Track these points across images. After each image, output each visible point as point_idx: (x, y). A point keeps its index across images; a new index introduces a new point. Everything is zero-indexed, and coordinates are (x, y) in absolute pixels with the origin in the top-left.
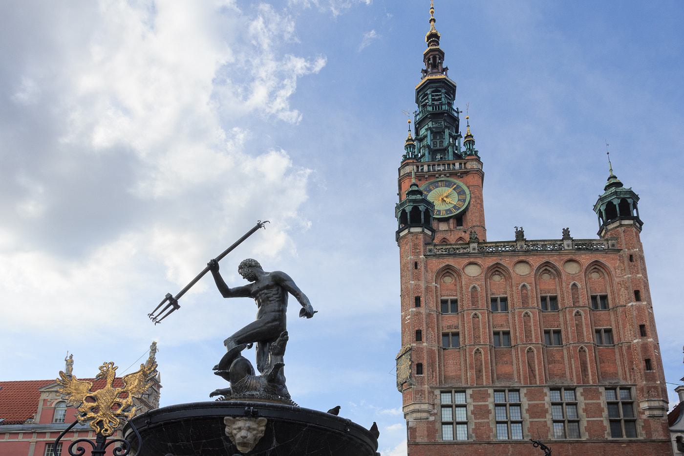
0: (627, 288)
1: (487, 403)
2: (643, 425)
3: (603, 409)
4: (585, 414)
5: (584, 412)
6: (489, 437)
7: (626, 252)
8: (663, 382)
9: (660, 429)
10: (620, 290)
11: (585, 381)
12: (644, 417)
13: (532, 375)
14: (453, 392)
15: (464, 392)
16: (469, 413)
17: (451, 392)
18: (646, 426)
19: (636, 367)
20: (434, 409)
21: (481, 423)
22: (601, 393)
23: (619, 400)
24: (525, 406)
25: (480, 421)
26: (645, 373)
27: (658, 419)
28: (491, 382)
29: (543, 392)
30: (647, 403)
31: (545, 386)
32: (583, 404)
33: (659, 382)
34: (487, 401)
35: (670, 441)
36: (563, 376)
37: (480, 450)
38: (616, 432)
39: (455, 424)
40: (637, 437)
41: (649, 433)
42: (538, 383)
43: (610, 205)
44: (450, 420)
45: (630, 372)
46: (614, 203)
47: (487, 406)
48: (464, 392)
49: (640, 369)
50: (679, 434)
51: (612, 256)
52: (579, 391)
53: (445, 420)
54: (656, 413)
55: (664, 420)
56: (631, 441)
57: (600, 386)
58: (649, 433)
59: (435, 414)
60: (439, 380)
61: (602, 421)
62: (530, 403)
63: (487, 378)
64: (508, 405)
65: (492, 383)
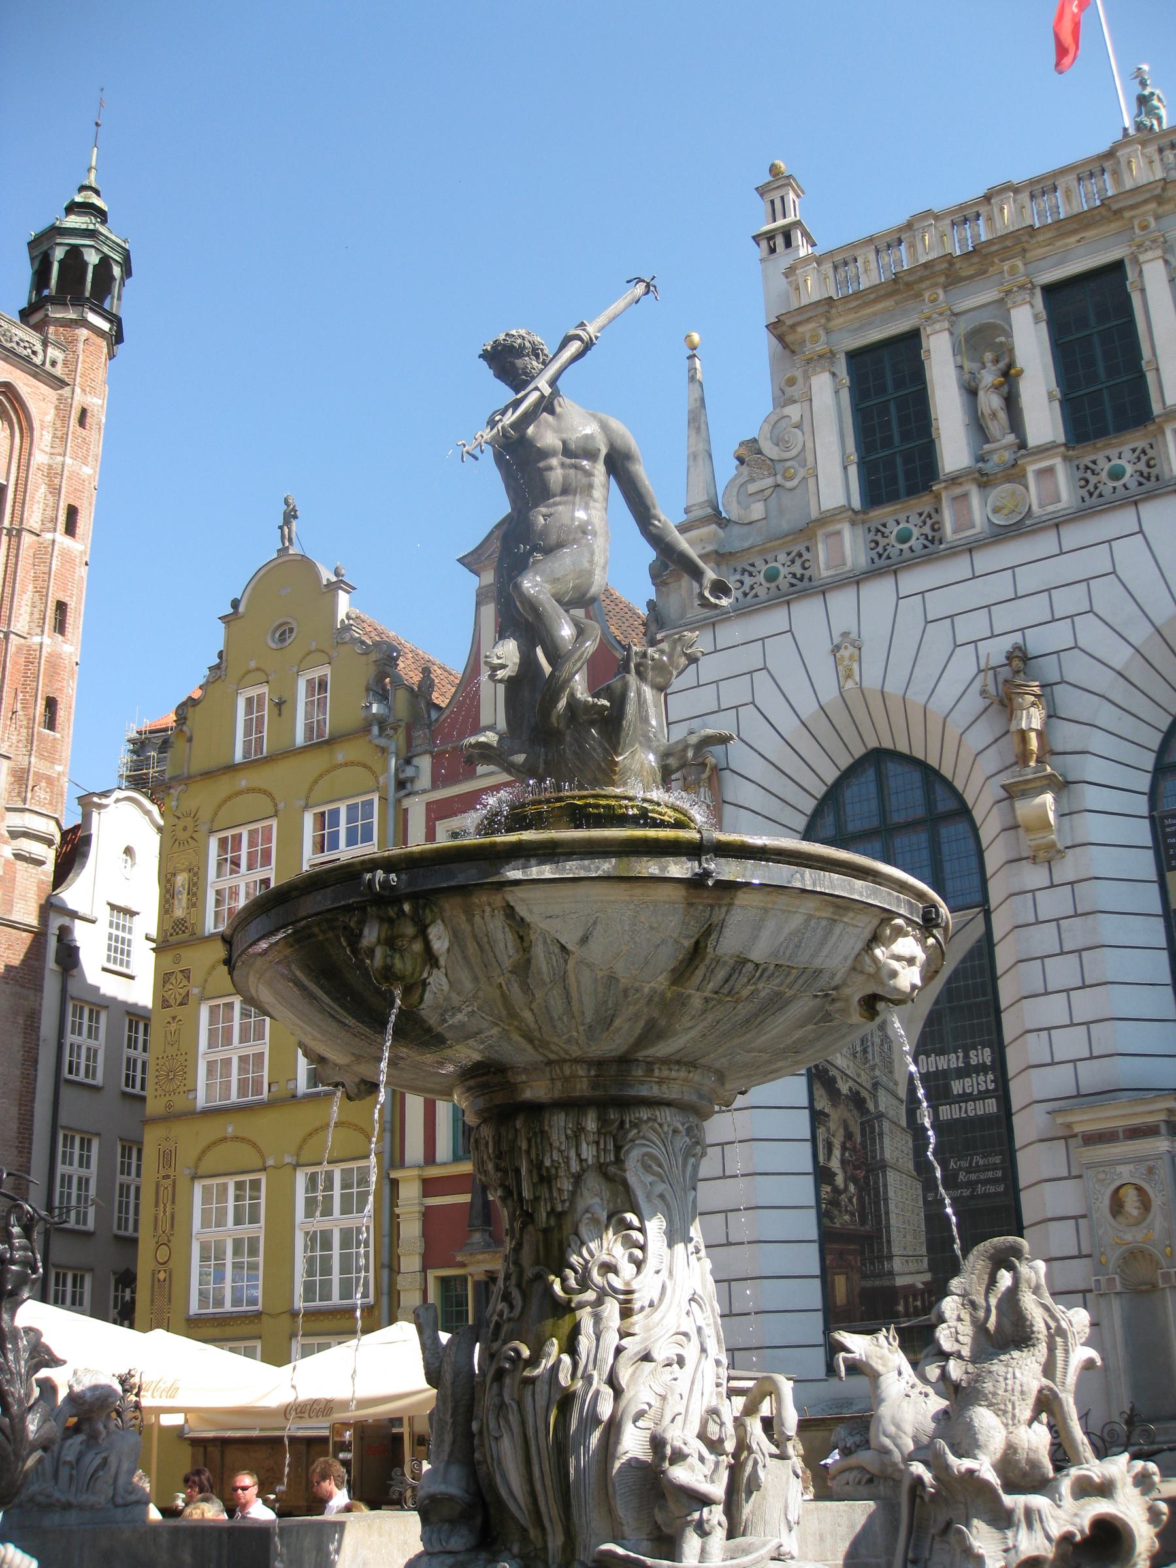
0: (56, 491)
7: (79, 399)
10: (37, 487)
33: (59, 768)
43: (75, 253)
46: (86, 258)
51: (44, 389)
55: (44, 873)
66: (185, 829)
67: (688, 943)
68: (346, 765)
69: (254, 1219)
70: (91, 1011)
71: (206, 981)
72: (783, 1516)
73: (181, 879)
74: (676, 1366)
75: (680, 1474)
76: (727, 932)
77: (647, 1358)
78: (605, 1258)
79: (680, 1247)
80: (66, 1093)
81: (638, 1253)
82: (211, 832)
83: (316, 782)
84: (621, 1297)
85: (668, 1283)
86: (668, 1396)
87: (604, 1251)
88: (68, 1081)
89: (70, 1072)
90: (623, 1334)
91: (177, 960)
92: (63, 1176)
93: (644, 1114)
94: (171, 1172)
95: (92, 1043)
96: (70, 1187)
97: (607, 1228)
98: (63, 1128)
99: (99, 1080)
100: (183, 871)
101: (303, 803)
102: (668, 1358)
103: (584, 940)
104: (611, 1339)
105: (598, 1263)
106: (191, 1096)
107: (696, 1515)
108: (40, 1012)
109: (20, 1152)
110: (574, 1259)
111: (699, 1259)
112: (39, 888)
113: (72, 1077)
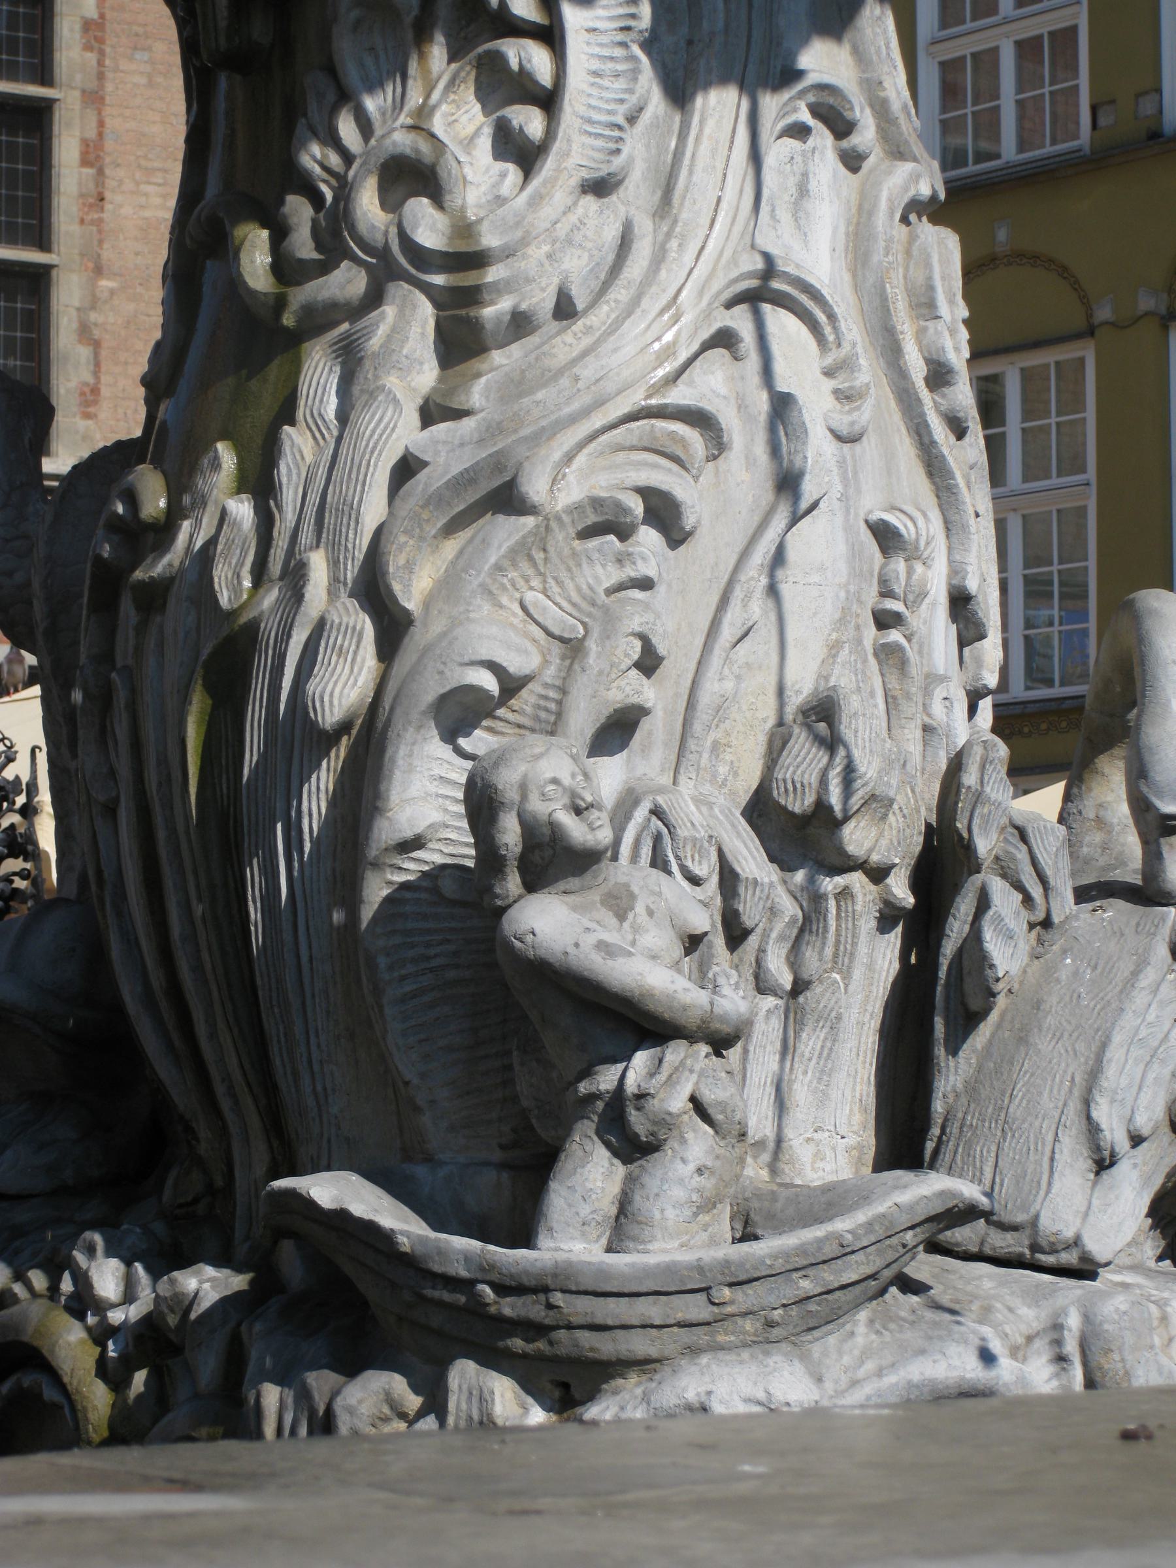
69: (1073, 463)
72: (1074, 1106)
74: (649, 538)
75: (548, 923)
77: (507, 499)
78: (401, 140)
79: (720, 106)
81: (531, 121)
84: (439, 280)
85: (644, 226)
86: (592, 645)
87: (404, 119)
90: (430, 414)
97: (421, 35)
102: (596, 503)
104: (394, 429)
105: (376, 161)
107: (606, 1079)
110: (314, 157)
111: (852, 161)
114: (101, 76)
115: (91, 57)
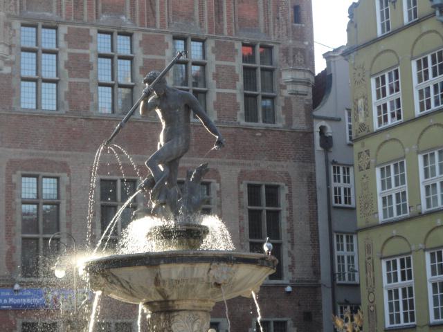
1: (87, 52)
2: (283, 105)
3: (238, 77)
4: (215, 81)
5: (213, 79)
6: (88, 108)
8: (311, 44)
9: (302, 113)
11: (219, 31)
12: (286, 93)
13: (151, 11)
14: (40, 26)
15: (56, 28)
16: (62, 66)
17: (36, 26)
18: (287, 109)
19: (283, 15)
20: (11, 53)
21: (77, 84)
22: (236, 51)
23: (258, 65)
24: (139, 62)
25: (76, 80)
26: (293, 26)
27: (301, 98)
28: (95, 17)
29: (164, 41)
30: (291, 73)
31: (167, 33)
32: (214, 66)
34: (88, 49)
35: (312, 132)
36: (190, 18)
37: (74, 129)
38: (250, 115)
39: (40, 81)
40: (274, 123)
41: (289, 120)
42: (158, 25)
44: (33, 74)
45: (274, 23)
47: (86, 56)
48: (56, 28)
49: (286, 20)
50: (323, 123)
52: (211, 44)
53: (25, 74)
54: (301, 88)
55: (307, 100)
56: (267, 129)
57: (236, 40)
58: (289, 120)
59: (11, 63)
60: (20, 4)
61: (234, 95)
62: (146, 57)
63: (90, 10)
64: (116, 58)
65: (97, 18)
66: (359, 75)
67: (154, 278)
68: (428, 32)
69: (410, 278)
70: (344, 168)
71: (377, 155)
73: (361, 102)
76: (162, 275)
80: (335, 214)
82: (372, 76)
83: (415, 43)
88: (335, 207)
89: (336, 202)
91: (363, 145)
92: (339, 257)
93: (175, 314)
94: (371, 256)
95: (347, 185)
96: (343, 262)
98: (336, 232)
99: (353, 205)
100: (361, 98)
101: (410, 56)
103: (130, 279)
106: (376, 216)
108: (315, 173)
109: (313, 247)
112: (305, 108)
113: (338, 205)
114: (221, 202)
115: (219, 198)
